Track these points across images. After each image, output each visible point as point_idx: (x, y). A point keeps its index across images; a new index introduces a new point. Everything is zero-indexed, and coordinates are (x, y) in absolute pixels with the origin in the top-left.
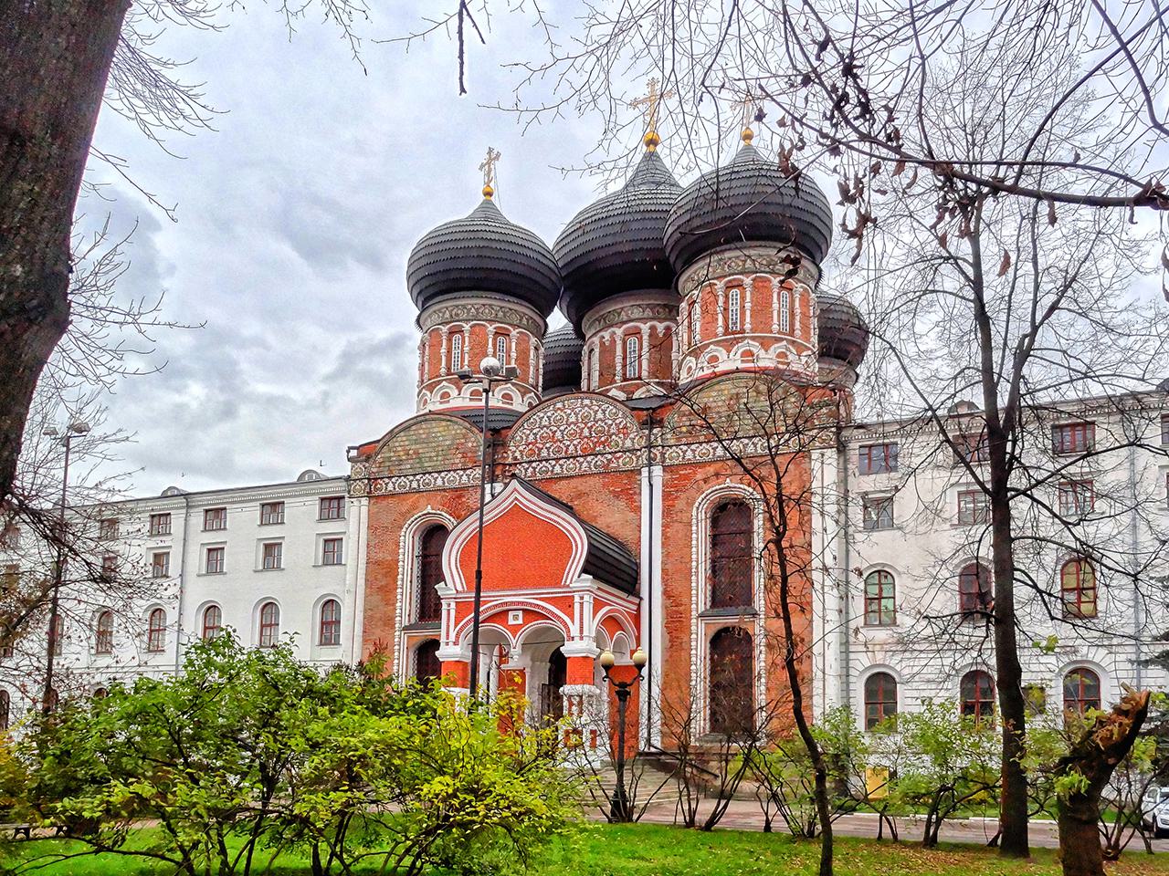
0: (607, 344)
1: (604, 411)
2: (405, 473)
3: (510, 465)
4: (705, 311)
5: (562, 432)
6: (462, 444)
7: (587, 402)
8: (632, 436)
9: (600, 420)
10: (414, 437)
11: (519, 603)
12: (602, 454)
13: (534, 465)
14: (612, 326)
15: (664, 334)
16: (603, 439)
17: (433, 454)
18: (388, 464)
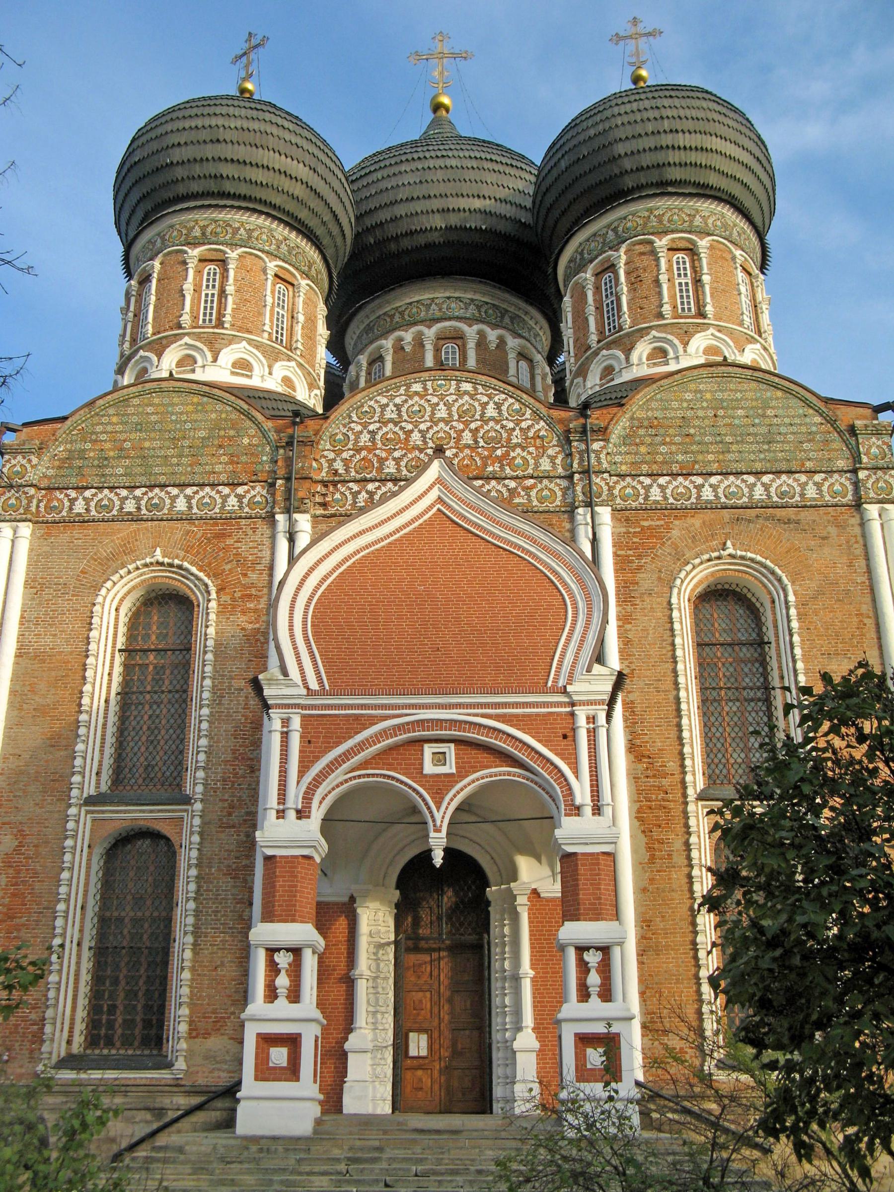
0: (408, 349)
1: (498, 406)
2: (112, 481)
3: (325, 484)
4: (635, 282)
5: (423, 433)
6: (230, 438)
7: (467, 387)
8: (550, 452)
9: (492, 419)
10: (135, 419)
11: (453, 723)
12: (499, 479)
13: (371, 487)
14: (415, 324)
15: (498, 346)
16: (499, 452)
17: (171, 452)
18: (78, 463)
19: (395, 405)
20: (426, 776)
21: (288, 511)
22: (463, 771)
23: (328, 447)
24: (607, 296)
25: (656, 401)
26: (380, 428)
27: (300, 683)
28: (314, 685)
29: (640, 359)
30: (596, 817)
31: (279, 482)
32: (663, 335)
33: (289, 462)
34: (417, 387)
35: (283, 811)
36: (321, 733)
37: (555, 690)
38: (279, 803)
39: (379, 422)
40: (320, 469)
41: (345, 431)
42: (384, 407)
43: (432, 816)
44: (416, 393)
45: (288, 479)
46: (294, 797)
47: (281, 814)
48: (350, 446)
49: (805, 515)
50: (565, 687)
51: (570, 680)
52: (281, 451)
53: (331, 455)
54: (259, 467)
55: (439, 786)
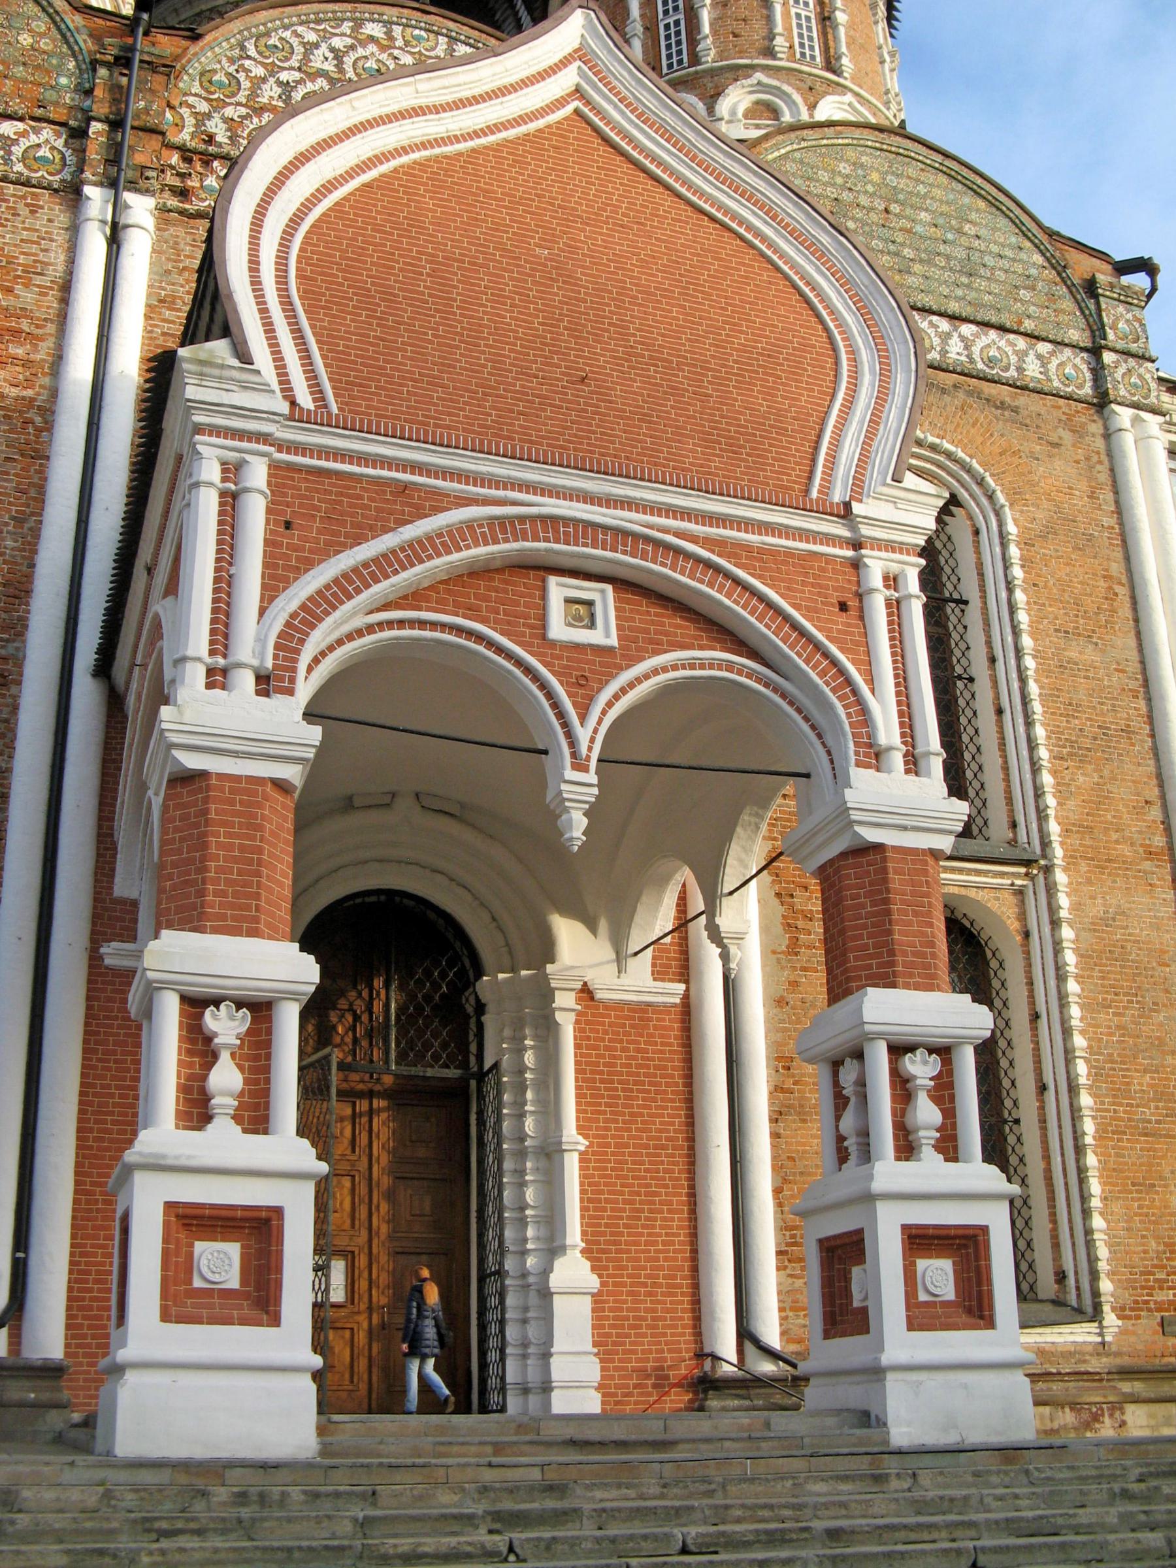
3: (186, 154)
11: (621, 536)
19: (332, 50)
20: (553, 644)
21: (112, 183)
22: (633, 647)
23: (196, 89)
24: (666, 12)
25: (794, 161)
26: (300, 82)
27: (275, 386)
28: (305, 400)
29: (733, 112)
30: (912, 777)
31: (96, 127)
32: (775, 83)
33: (120, 96)
34: (374, 29)
35: (224, 672)
36: (316, 512)
37: (823, 510)
38: (212, 653)
39: (300, 69)
40: (179, 126)
41: (232, 69)
42: (310, 47)
43: (569, 735)
44: (372, 39)
45: (116, 124)
46: (253, 641)
47: (218, 678)
48: (241, 97)
49: (1023, 400)
50: (847, 506)
51: (858, 489)
52: (103, 72)
53: (203, 107)
54: (50, 95)
55: (587, 670)
